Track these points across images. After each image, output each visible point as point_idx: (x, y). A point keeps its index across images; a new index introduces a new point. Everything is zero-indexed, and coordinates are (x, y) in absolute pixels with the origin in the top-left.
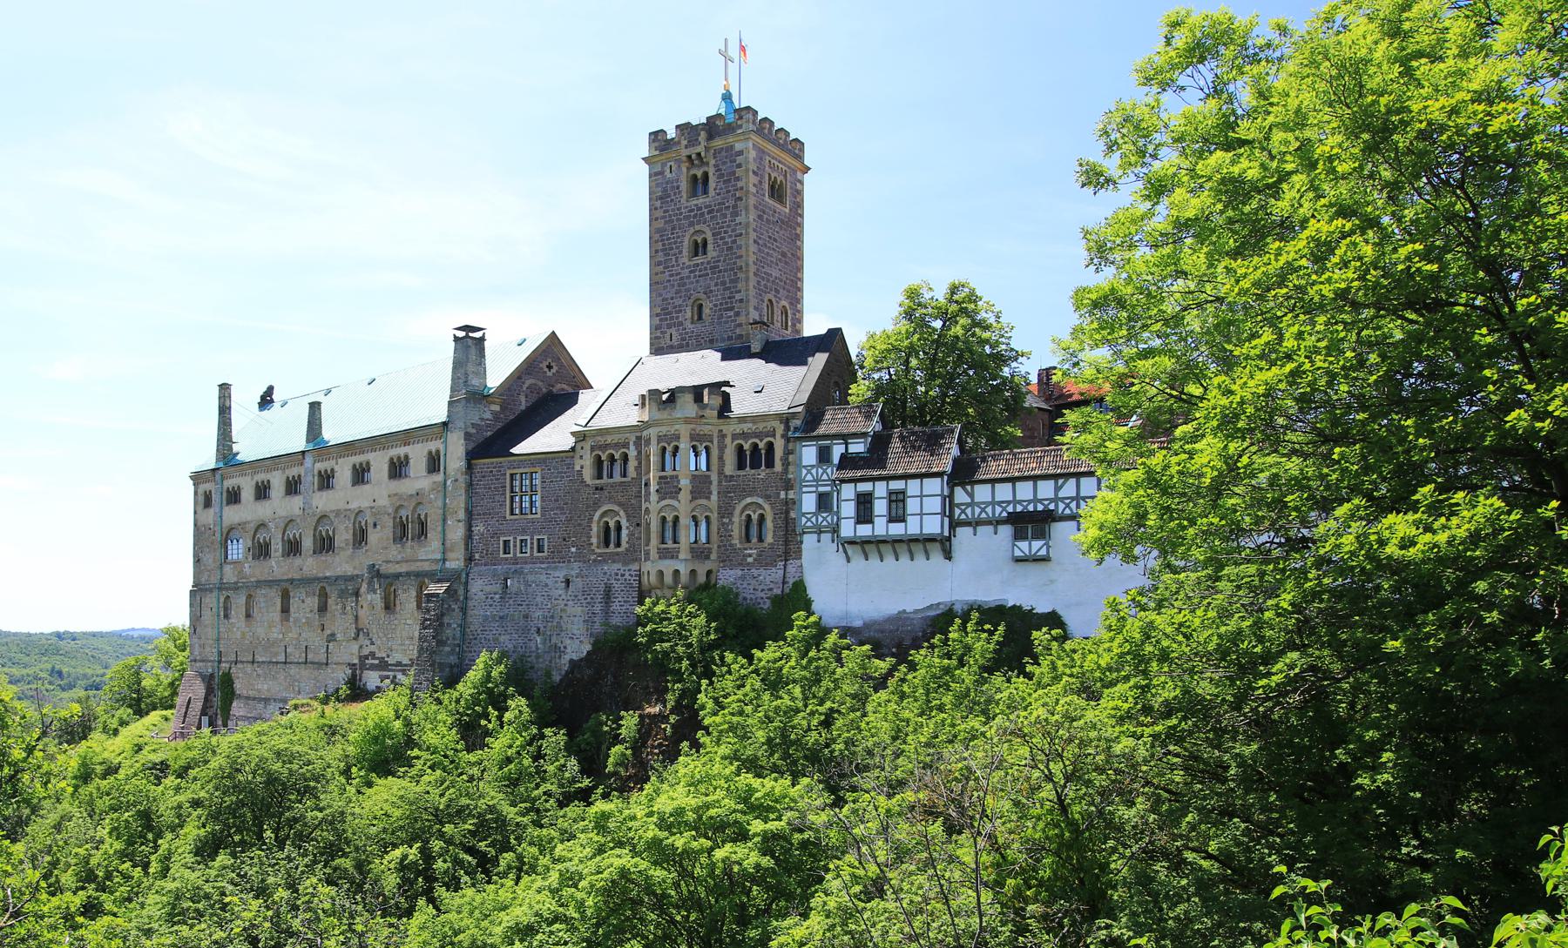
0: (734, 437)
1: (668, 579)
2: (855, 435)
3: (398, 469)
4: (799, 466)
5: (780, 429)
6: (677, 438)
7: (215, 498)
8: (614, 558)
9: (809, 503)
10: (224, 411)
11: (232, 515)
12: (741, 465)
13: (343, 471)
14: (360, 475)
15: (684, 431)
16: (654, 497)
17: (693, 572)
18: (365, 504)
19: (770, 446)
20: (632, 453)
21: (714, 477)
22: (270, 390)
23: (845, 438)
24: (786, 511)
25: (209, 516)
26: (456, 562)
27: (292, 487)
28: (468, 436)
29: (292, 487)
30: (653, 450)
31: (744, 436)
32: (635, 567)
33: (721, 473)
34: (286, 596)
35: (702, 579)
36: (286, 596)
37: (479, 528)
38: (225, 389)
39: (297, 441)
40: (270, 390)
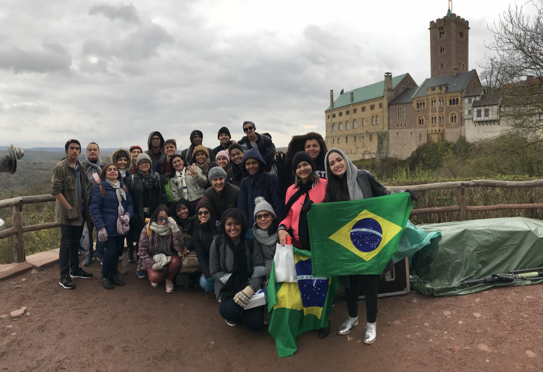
0: (449, 97)
1: (434, 132)
2: (477, 96)
3: (372, 107)
4: (464, 104)
5: (460, 95)
6: (435, 98)
7: (330, 116)
8: (421, 127)
9: (466, 112)
10: (332, 96)
11: (334, 120)
12: (451, 104)
13: (359, 108)
14: (363, 109)
15: (437, 96)
16: (430, 113)
17: (439, 130)
18: (364, 117)
19: (457, 99)
20: (425, 102)
21: (444, 107)
22: (343, 91)
23: (475, 96)
24: (461, 114)
25: (329, 121)
26: (386, 129)
27: (348, 113)
28: (388, 99)
29: (348, 113)
30: (430, 101)
31: (451, 97)
32: (426, 129)
33: (446, 106)
34: (347, 137)
35: (441, 131)
36: (347, 137)
37: (391, 121)
38: (332, 91)
39: (349, 103)
40: (343, 91)
